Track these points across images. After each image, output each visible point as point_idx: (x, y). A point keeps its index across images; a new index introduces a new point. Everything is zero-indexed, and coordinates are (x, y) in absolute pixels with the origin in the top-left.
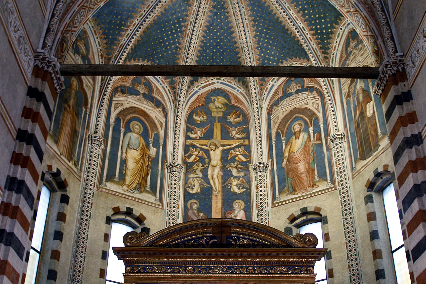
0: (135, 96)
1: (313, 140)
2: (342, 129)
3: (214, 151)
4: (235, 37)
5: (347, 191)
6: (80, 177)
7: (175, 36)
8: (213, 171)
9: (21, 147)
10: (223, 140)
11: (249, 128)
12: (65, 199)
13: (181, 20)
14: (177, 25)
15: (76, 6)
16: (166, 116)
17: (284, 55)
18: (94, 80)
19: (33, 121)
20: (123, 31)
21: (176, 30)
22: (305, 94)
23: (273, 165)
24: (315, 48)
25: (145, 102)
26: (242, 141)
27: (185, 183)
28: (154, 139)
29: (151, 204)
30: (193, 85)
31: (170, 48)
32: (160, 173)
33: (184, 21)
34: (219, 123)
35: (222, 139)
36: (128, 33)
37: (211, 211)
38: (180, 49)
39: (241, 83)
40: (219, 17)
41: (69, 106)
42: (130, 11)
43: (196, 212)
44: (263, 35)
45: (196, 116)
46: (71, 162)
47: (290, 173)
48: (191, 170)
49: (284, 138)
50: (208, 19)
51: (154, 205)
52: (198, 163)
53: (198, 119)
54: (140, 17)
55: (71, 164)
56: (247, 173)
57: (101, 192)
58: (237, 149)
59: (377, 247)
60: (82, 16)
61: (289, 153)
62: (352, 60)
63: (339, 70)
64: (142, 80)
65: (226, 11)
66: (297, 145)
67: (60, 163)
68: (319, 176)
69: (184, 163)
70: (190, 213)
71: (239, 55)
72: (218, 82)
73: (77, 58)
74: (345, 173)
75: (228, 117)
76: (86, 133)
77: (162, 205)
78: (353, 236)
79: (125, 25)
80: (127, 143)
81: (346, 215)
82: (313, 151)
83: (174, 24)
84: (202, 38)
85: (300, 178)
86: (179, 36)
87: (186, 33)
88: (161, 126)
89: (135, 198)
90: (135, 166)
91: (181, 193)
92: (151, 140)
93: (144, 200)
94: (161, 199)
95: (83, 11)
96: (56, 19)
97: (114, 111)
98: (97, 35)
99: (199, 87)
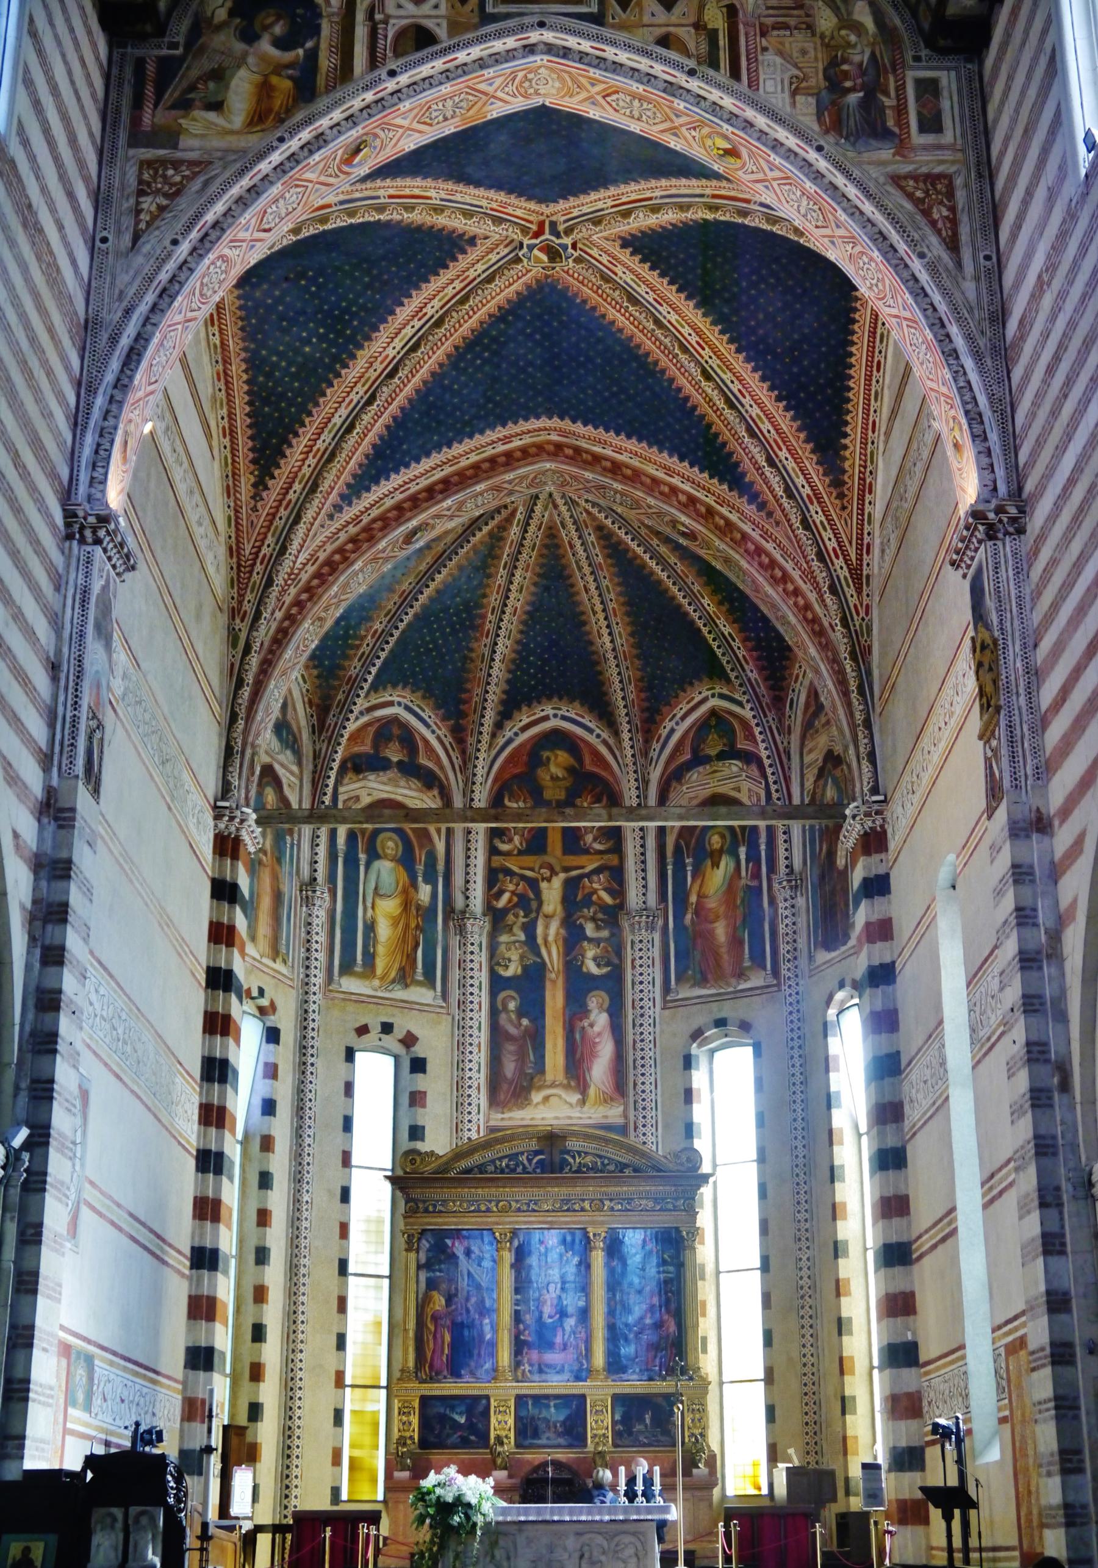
3: (549, 880)
8: (547, 927)
9: (215, 1000)
19: (227, 946)
22: (734, 766)
25: (403, 783)
26: (606, 857)
28: (426, 865)
32: (440, 938)
38: (472, 661)
43: (513, 1016)
47: (699, 941)
55: (279, 966)
57: (333, 999)
58: (595, 878)
61: (699, 896)
68: (751, 958)
70: (503, 1018)
72: (555, 716)
79: (356, 637)
80: (372, 885)
82: (743, 901)
84: (519, 636)
91: (484, 977)
92: (420, 868)
94: (445, 995)
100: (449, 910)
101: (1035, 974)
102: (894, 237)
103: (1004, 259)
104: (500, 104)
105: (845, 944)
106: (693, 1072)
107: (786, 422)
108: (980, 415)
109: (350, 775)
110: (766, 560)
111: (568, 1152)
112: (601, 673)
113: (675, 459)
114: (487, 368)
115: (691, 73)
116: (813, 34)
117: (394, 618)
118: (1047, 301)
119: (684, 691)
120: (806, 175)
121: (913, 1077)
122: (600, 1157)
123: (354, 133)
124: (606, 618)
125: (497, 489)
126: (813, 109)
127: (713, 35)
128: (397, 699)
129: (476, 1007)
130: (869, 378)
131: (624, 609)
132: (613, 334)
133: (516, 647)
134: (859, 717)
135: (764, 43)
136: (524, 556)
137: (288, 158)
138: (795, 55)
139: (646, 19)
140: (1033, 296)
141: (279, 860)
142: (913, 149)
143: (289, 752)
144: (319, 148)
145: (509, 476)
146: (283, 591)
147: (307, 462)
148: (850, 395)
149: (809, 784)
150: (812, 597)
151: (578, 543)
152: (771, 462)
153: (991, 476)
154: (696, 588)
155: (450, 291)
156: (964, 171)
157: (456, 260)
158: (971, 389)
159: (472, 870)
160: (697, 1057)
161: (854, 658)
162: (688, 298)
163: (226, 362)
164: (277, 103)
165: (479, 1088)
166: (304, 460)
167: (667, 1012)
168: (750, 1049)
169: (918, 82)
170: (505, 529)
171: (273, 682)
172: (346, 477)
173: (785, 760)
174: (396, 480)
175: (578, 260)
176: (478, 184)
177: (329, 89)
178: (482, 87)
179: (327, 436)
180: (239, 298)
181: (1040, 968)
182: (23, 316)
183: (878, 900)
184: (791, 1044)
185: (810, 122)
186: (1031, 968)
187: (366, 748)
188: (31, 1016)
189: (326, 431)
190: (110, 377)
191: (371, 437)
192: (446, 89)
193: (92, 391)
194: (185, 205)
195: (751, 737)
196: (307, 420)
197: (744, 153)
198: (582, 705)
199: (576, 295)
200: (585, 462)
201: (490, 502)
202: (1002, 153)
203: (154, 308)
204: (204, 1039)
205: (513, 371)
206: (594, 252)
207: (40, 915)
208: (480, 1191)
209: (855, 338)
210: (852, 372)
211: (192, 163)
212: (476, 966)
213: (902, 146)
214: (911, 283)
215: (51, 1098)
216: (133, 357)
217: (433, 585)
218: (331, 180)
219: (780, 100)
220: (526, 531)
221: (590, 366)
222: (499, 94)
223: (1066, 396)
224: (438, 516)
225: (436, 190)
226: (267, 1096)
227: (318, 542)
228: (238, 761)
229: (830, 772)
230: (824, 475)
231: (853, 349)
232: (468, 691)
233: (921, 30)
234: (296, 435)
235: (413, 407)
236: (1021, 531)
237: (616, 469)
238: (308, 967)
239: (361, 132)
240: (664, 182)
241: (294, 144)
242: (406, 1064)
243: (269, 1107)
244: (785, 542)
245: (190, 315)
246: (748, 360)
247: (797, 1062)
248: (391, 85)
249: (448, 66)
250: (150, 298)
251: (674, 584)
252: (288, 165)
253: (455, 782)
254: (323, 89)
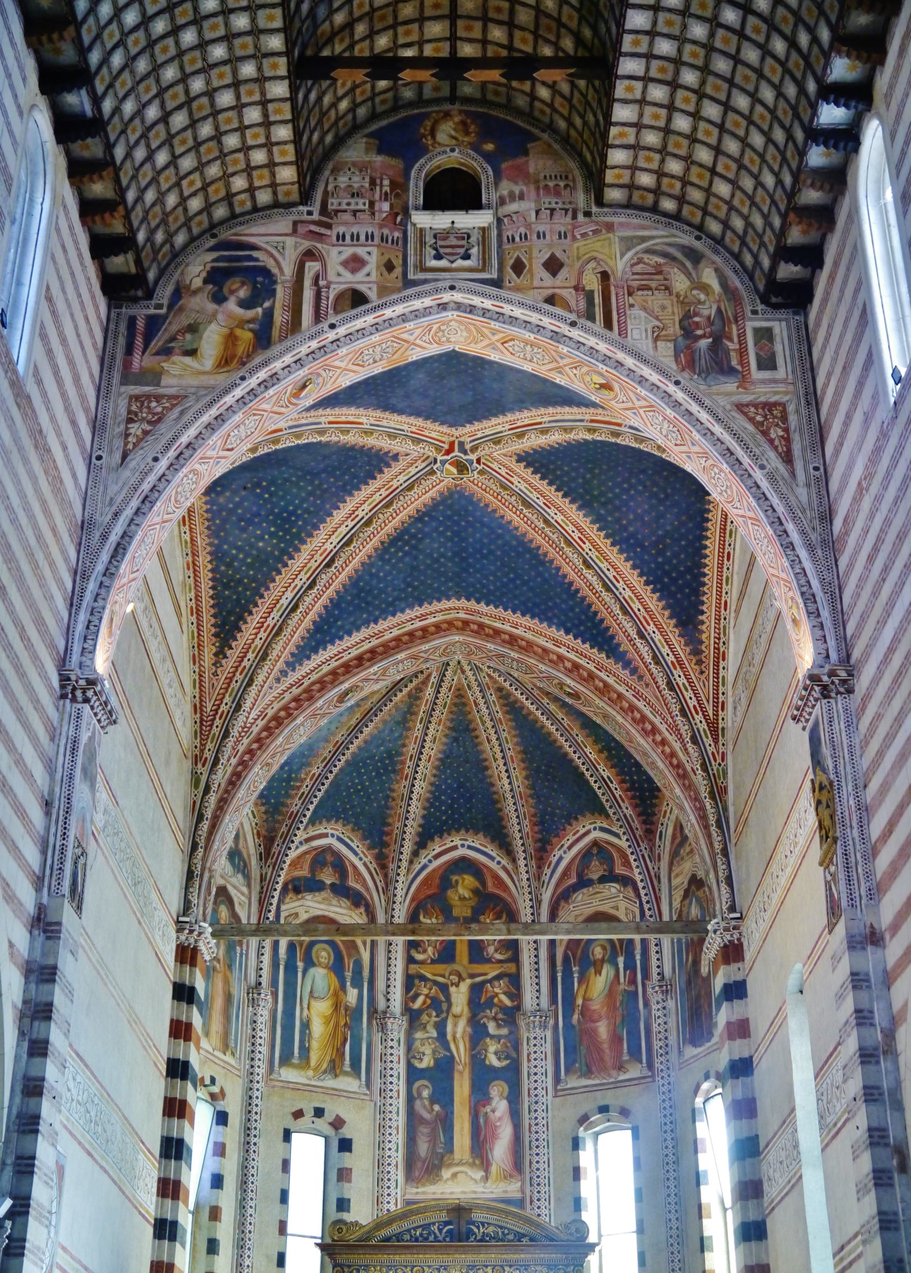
1: (623, 985)
3: (457, 985)
4: (491, 777)
8: (455, 1025)
9: (173, 1087)
21: (386, 769)
22: (613, 888)
25: (334, 902)
26: (505, 965)
32: (365, 1034)
33: (399, 754)
38: (394, 800)
40: (461, 743)
43: (427, 1103)
50: (441, 747)
51: (357, 1096)
52: (430, 1010)
55: (228, 1058)
57: (274, 1087)
58: (496, 983)
61: (584, 999)
62: (688, 854)
65: (473, 734)
68: (630, 1052)
70: (418, 1104)
71: (499, 806)
72: (463, 846)
80: (308, 989)
81: (665, 1132)
82: (621, 1003)
84: (433, 779)
85: (600, 1050)
91: (402, 1068)
92: (348, 974)
94: (368, 1085)
100: (373, 1011)
101: (872, 1068)
102: (740, 452)
103: (829, 470)
104: (419, 349)
105: (709, 1040)
106: (581, 1152)
107: (654, 602)
108: (814, 595)
109: (291, 895)
110: (638, 716)
111: (473, 1223)
112: (501, 810)
113: (562, 632)
114: (407, 559)
115: (573, 324)
116: (671, 294)
117: (329, 763)
118: (866, 503)
119: (571, 825)
120: (667, 404)
121: (770, 1158)
122: (501, 1227)
123: (302, 373)
124: (505, 764)
125: (415, 657)
126: (671, 352)
127: (590, 296)
128: (330, 831)
129: (395, 1094)
130: (721, 566)
131: (520, 756)
132: (510, 531)
133: (430, 788)
134: (718, 847)
135: (631, 301)
136: (437, 713)
137: (248, 393)
138: (656, 310)
139: (536, 283)
140: (854, 499)
141: (230, 967)
142: (752, 383)
143: (240, 876)
144: (273, 385)
145: (426, 647)
146: (238, 741)
147: (259, 636)
148: (706, 580)
149: (676, 904)
150: (677, 746)
151: (481, 702)
152: (641, 636)
153: (824, 646)
154: (580, 739)
155: (377, 498)
156: (795, 401)
157: (381, 472)
158: (805, 575)
159: (392, 976)
160: (584, 1139)
161: (712, 796)
162: (571, 502)
163: (195, 554)
164: (241, 349)
165: (397, 1166)
166: (256, 634)
167: (558, 1099)
168: (629, 1132)
169: (756, 331)
170: (421, 691)
171: (227, 817)
172: (291, 648)
173: (656, 883)
174: (332, 650)
175: (482, 472)
176: (400, 412)
177: (281, 341)
178: (405, 336)
179: (276, 614)
180: (206, 503)
181: (878, 1063)
182: (32, 518)
183: (736, 1002)
184: (664, 1128)
185: (670, 363)
186: (870, 1062)
187: (304, 872)
188: (18, 1100)
189: (275, 610)
190: (100, 567)
191: (312, 615)
192: (376, 338)
193: (85, 577)
194: (165, 430)
195: (627, 864)
196: (260, 602)
197: (616, 387)
198: (485, 837)
199: (480, 500)
200: (488, 635)
201: (410, 668)
202: (826, 385)
203: (137, 512)
204: (163, 1121)
205: (428, 562)
206: (495, 466)
207: (29, 1013)
208: (397, 1257)
209: (709, 534)
210: (706, 561)
211: (170, 397)
212: (395, 1059)
213: (744, 380)
214: (754, 489)
215: (32, 1173)
216: (119, 550)
217: (361, 737)
218: (283, 410)
219: (645, 345)
220: (439, 692)
221: (492, 558)
222: (418, 342)
223: (884, 580)
224: (367, 680)
225: (366, 417)
226: (216, 1172)
227: (266, 701)
228: (197, 883)
229: (694, 893)
230: (686, 645)
231: (708, 543)
232: (389, 825)
233: (757, 291)
234: (251, 613)
235: (346, 590)
236: (850, 691)
237: (512, 641)
238: (252, 1059)
239: (307, 372)
240: (551, 410)
241: (253, 382)
242: (335, 1144)
243: (217, 1181)
244: (653, 700)
245: (166, 517)
246: (621, 551)
247: (670, 1144)
248: (331, 335)
249: (376, 320)
250: (135, 503)
251: (562, 735)
252: (247, 398)
253: (378, 902)
254: (277, 339)
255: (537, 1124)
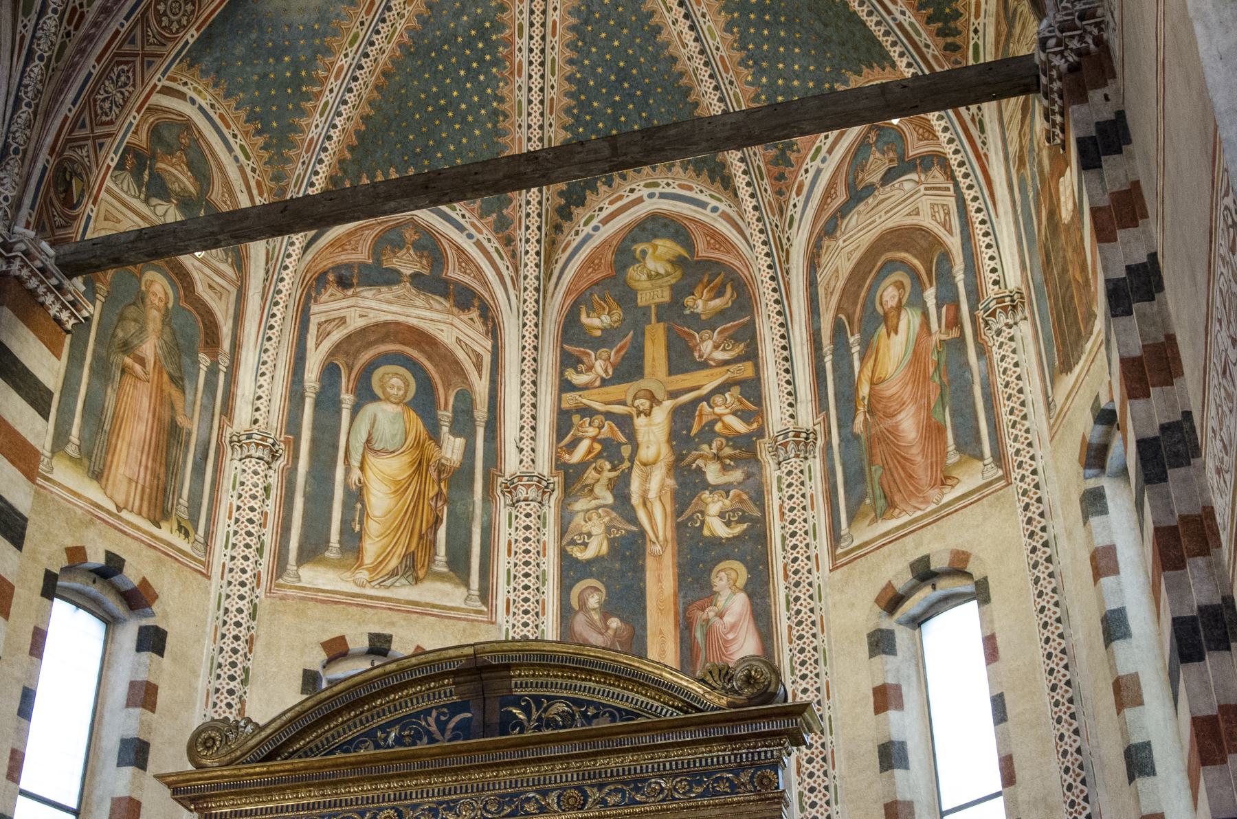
0: (384, 289)
1: (938, 332)
2: (1013, 279)
3: (648, 414)
4: (668, 44)
5: (1037, 486)
6: (208, 564)
7: (482, 78)
8: (646, 479)
10: (673, 378)
11: (754, 323)
12: (153, 641)
13: (487, 25)
14: (480, 45)
15: (92, 61)
16: (494, 331)
17: (832, 66)
18: (240, 264)
20: (311, 100)
21: (481, 61)
22: (908, 182)
23: (830, 433)
24: (911, 24)
25: (419, 301)
26: (733, 368)
27: (563, 532)
28: (455, 411)
29: (452, 614)
30: (571, 219)
31: (475, 120)
32: (478, 511)
34: (662, 324)
35: (671, 372)
36: (324, 100)
37: (644, 608)
38: (506, 116)
39: (718, 184)
41: (142, 361)
42: (315, 34)
43: (596, 617)
44: (752, 16)
45: (588, 316)
46: (164, 524)
47: (877, 451)
48: (579, 486)
49: (857, 336)
52: (600, 462)
53: (595, 322)
54: (351, 44)
56: (754, 470)
58: (718, 399)
59: (1124, 669)
60: (125, 85)
63: (898, 90)
64: (407, 235)
66: (892, 352)
67: (119, 534)
68: (959, 448)
69: (557, 467)
70: (580, 624)
71: (692, 98)
72: (651, 196)
73: (160, 210)
74: (1027, 424)
75: (689, 301)
76: (221, 428)
77: (492, 610)
78: (1061, 636)
79: (313, 81)
80: (364, 437)
83: (470, 42)
84: (569, 69)
85: (904, 461)
86: (495, 77)
87: (512, 63)
88: (479, 367)
89: (398, 601)
90: (393, 503)
91: (551, 564)
92: (445, 415)
93: (427, 605)
94: (485, 594)
95: (123, 71)
96: (24, 113)
97: (317, 346)
98: (233, 127)
99: (595, 222)
111: (516, 702)
173: (975, 132)
255: (800, 623)
